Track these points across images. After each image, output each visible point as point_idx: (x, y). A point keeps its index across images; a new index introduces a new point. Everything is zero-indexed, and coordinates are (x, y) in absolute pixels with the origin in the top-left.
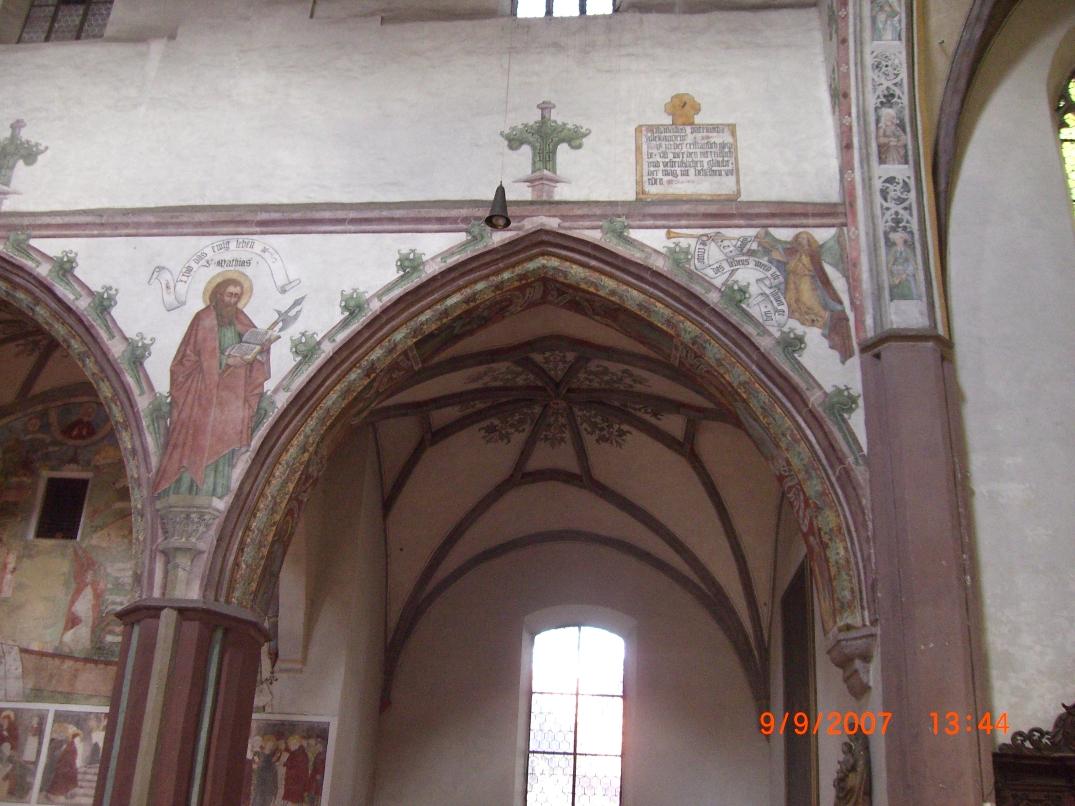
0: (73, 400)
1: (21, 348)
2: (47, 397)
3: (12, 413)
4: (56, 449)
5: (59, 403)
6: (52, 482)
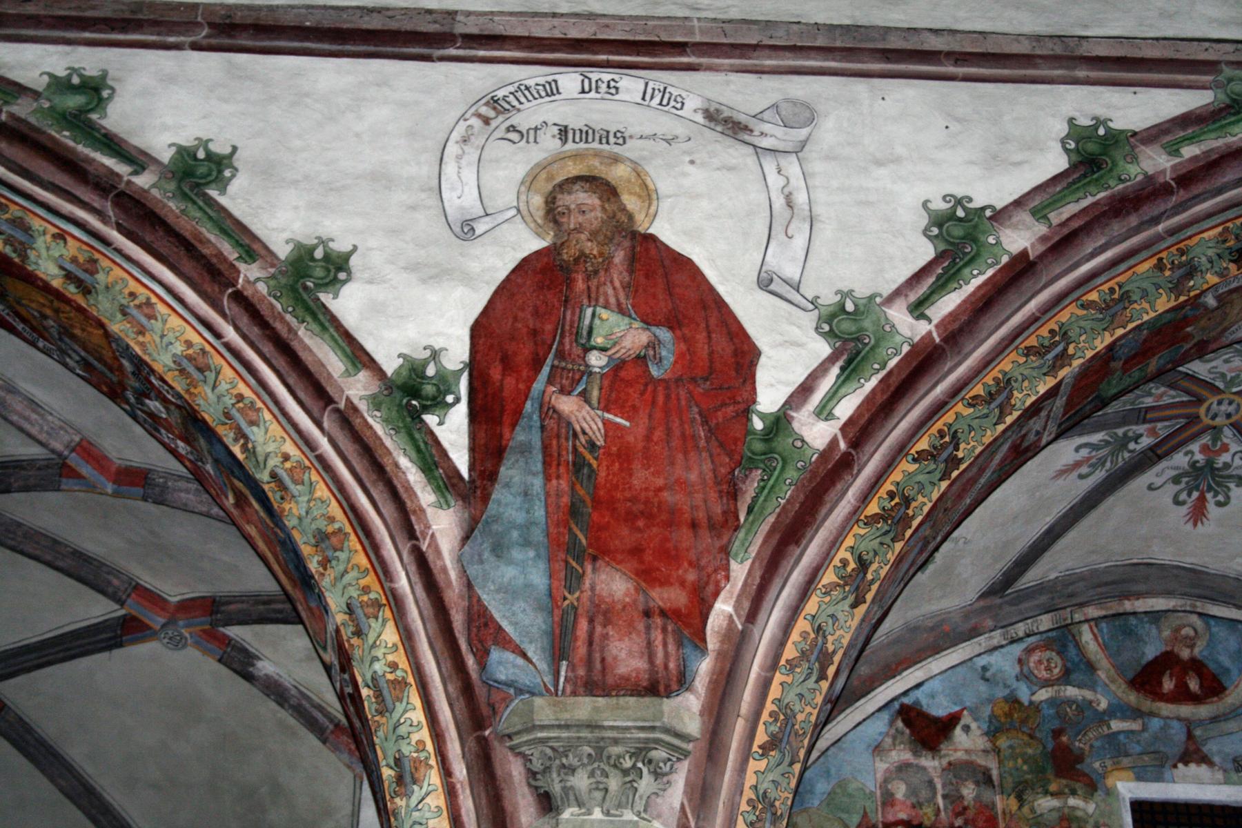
0: (1128, 606)
1: (1084, 452)
2: (1060, 595)
3: (973, 633)
4: (1135, 726)
5: (1093, 612)
6: (1139, 807)
